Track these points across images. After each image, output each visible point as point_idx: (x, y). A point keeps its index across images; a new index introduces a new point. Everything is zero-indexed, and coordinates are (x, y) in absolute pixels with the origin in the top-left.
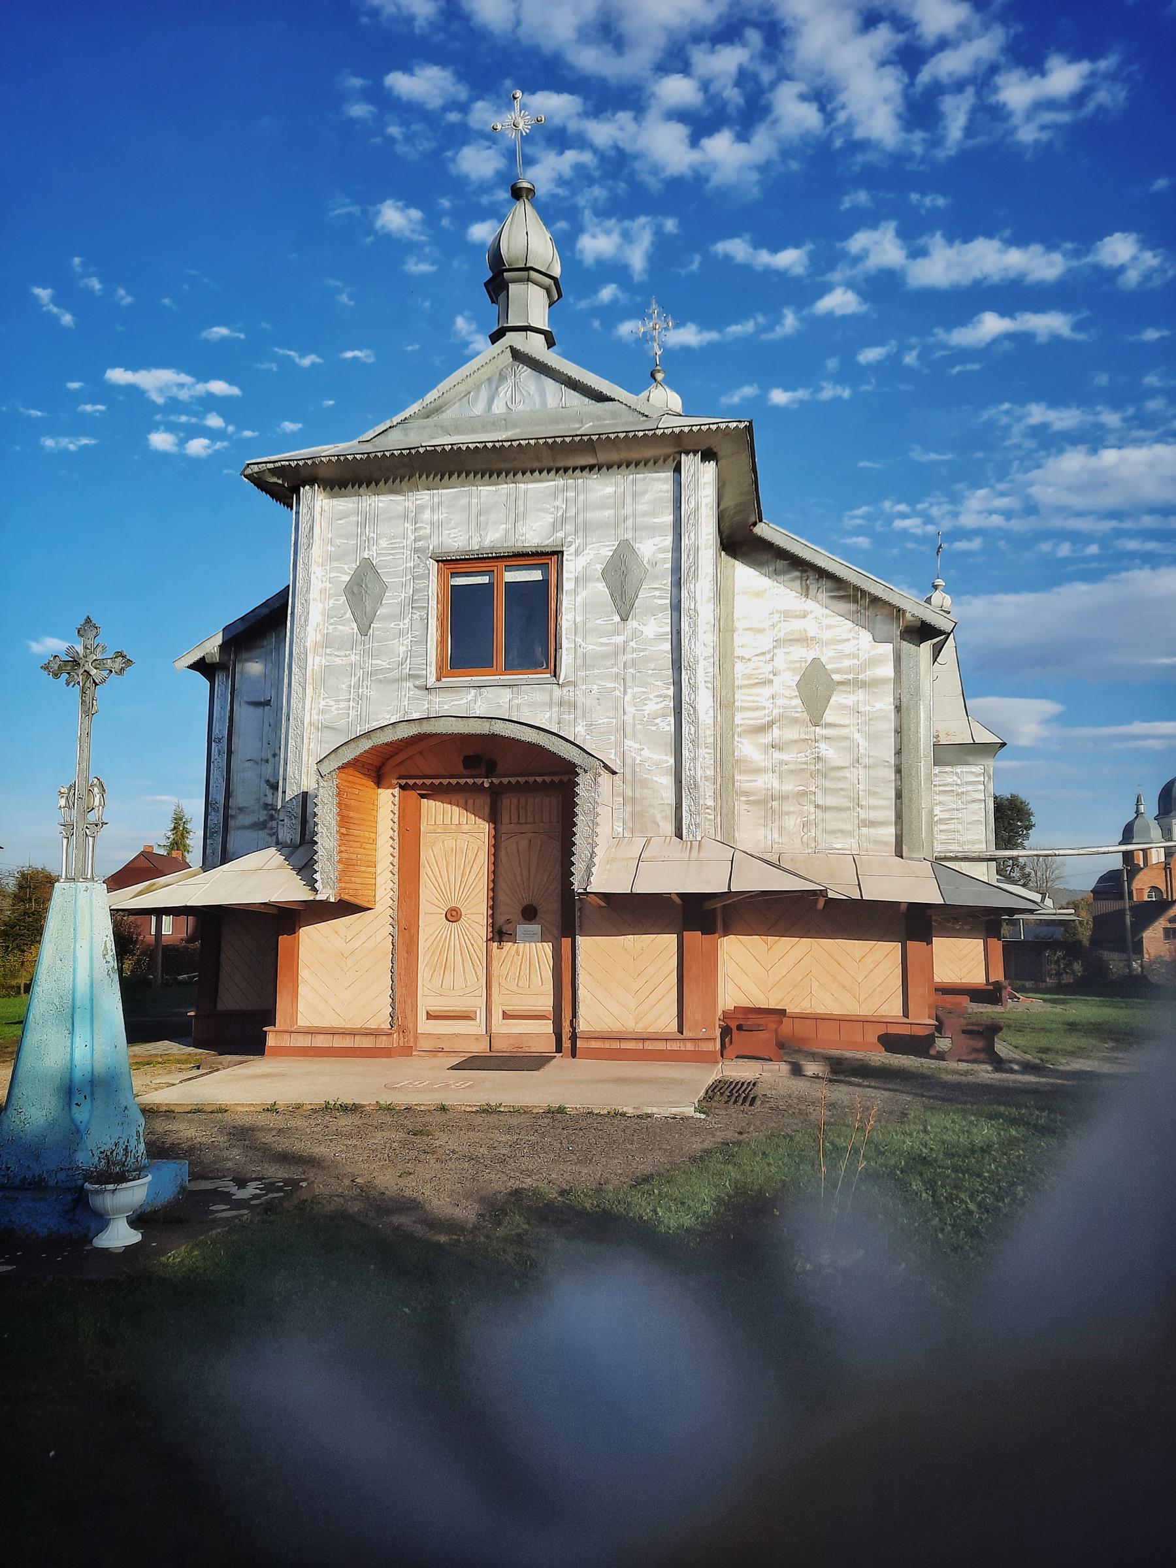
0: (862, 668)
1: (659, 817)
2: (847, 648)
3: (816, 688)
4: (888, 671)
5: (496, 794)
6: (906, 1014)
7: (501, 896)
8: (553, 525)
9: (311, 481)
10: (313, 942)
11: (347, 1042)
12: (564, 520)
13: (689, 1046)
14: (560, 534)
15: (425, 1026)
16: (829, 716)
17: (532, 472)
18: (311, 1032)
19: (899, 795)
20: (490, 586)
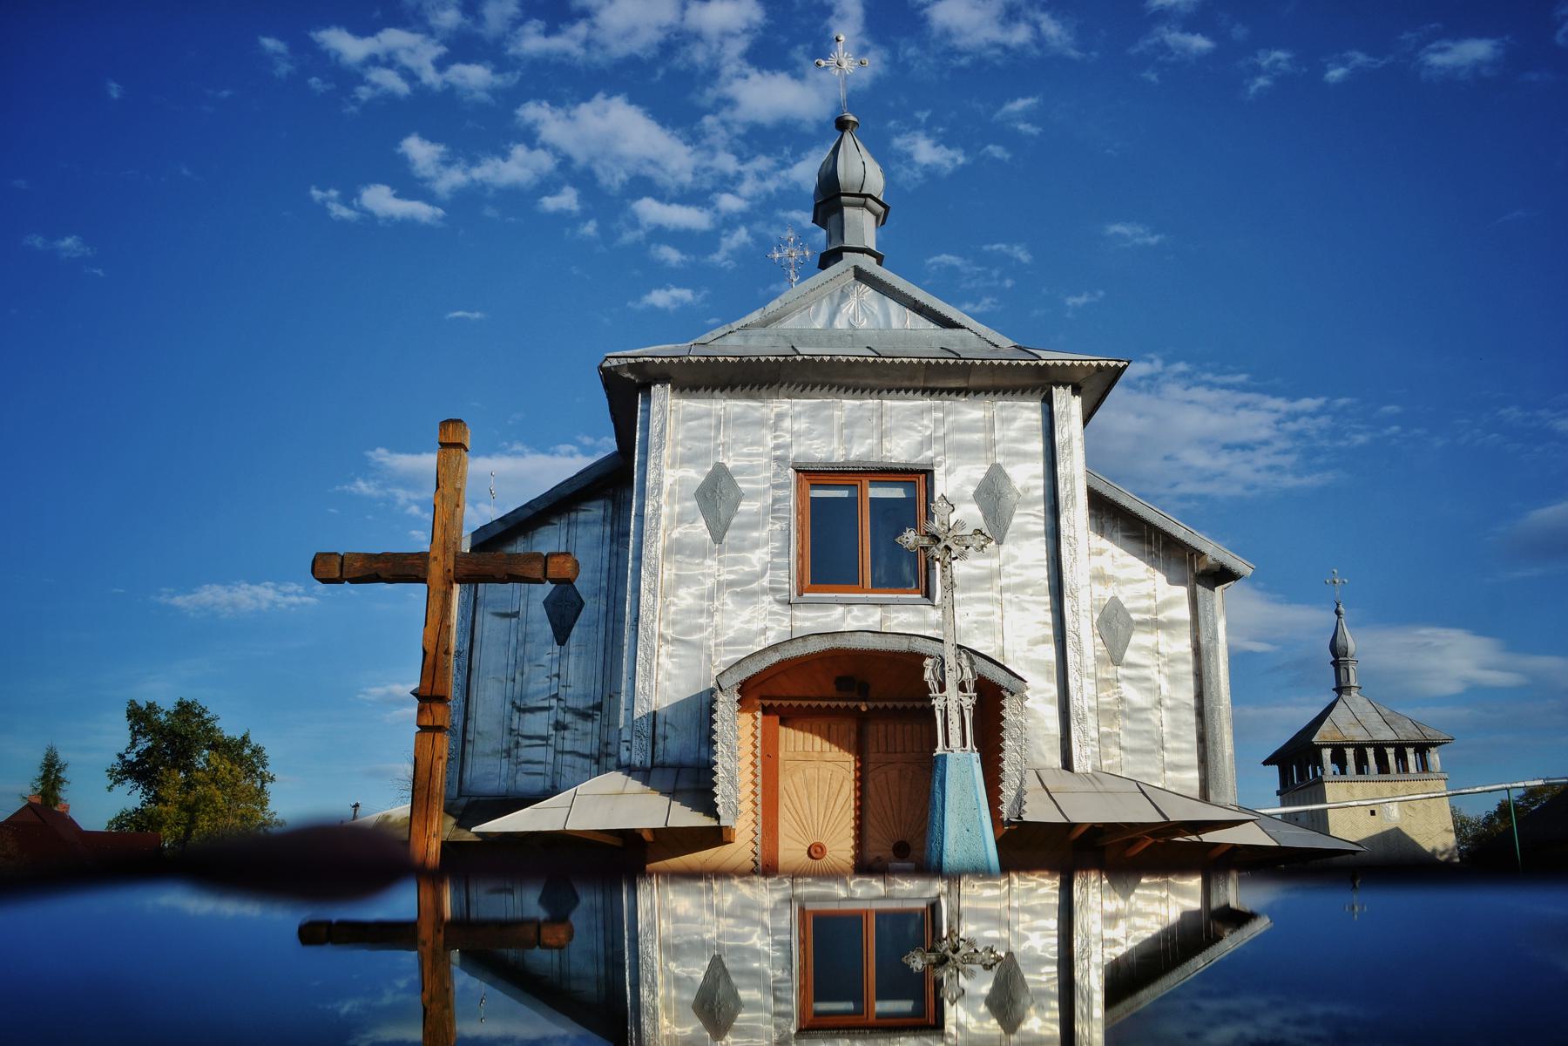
0: (1159, 609)
1: (1045, 748)
2: (1144, 588)
4: (1183, 612)
5: (862, 720)
7: (871, 831)
8: (921, 443)
9: (663, 378)
12: (929, 442)
14: (930, 454)
16: (1130, 656)
17: (898, 391)
19: (1202, 739)
20: (852, 503)
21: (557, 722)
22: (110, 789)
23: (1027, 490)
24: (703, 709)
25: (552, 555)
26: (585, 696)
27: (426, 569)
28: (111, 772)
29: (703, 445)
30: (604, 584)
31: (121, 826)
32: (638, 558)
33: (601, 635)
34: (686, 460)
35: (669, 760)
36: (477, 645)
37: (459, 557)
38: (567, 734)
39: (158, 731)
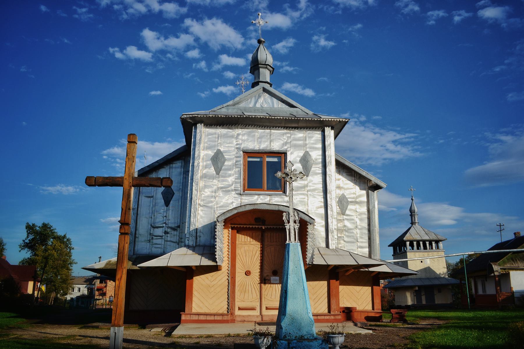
0: (357, 198)
1: (320, 241)
2: (352, 191)
4: (365, 199)
5: (263, 232)
6: (373, 309)
7: (265, 267)
8: (283, 144)
10: (199, 282)
11: (212, 318)
12: (286, 143)
13: (332, 317)
14: (286, 147)
15: (237, 312)
16: (347, 212)
17: (276, 127)
18: (199, 314)
19: (370, 239)
20: (261, 163)
21: (165, 231)
22: (20, 251)
23: (316, 159)
24: (212, 228)
25: (164, 178)
26: (175, 223)
27: (123, 183)
28: (20, 246)
29: (213, 144)
30: (181, 187)
31: (23, 263)
32: (192, 179)
33: (180, 203)
34: (209, 148)
35: (201, 244)
36: (140, 206)
37: (134, 178)
38: (168, 235)
39: (36, 233)
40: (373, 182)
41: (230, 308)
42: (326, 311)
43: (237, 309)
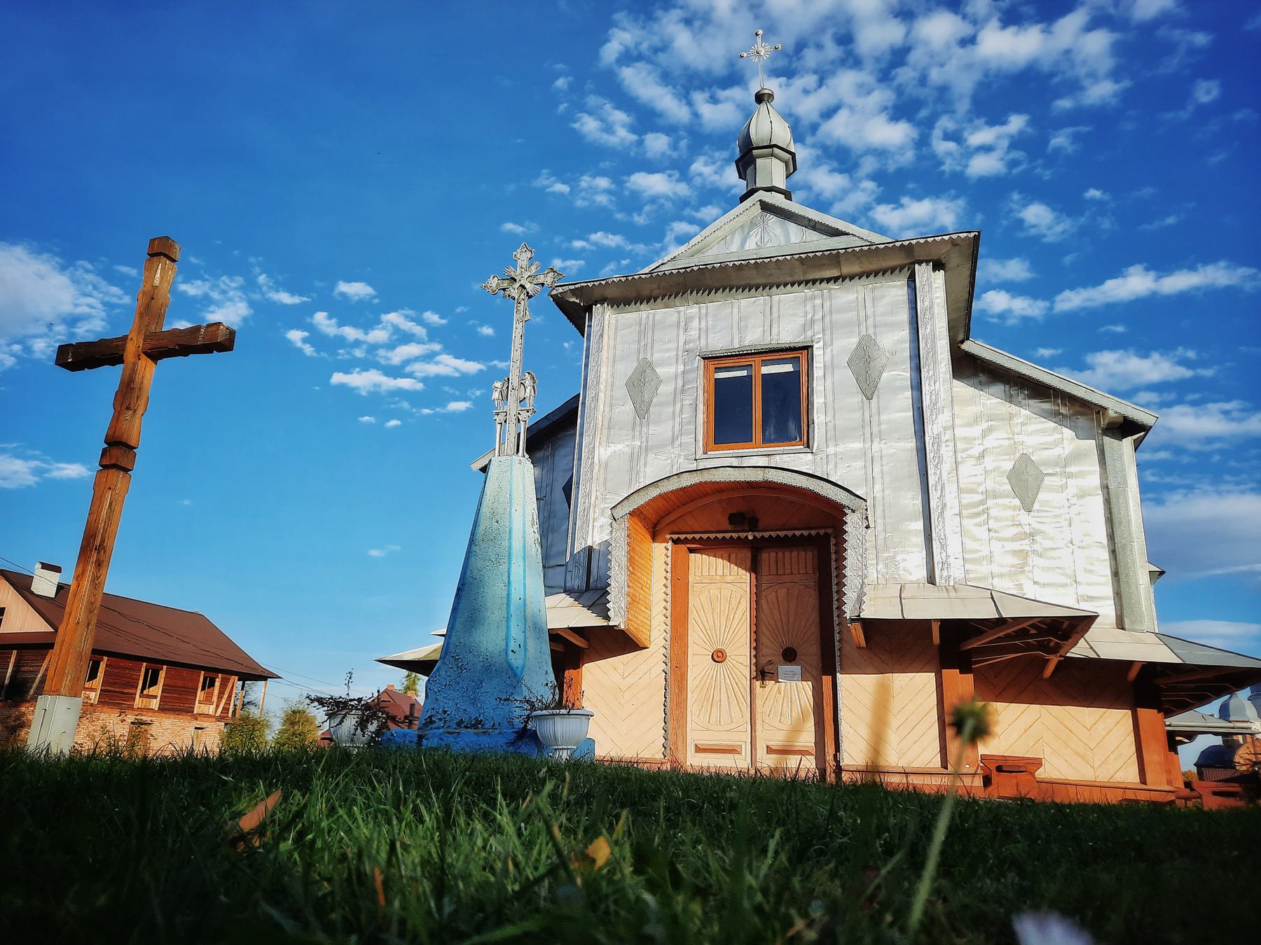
3: (1025, 482)
6: (1143, 781)
7: (764, 640)
9: (602, 301)
12: (813, 321)
14: (809, 333)
17: (785, 285)
19: (1116, 574)
20: (749, 377)
23: (894, 353)
40: (1111, 413)
41: (670, 743)
42: (936, 762)
43: (691, 749)
